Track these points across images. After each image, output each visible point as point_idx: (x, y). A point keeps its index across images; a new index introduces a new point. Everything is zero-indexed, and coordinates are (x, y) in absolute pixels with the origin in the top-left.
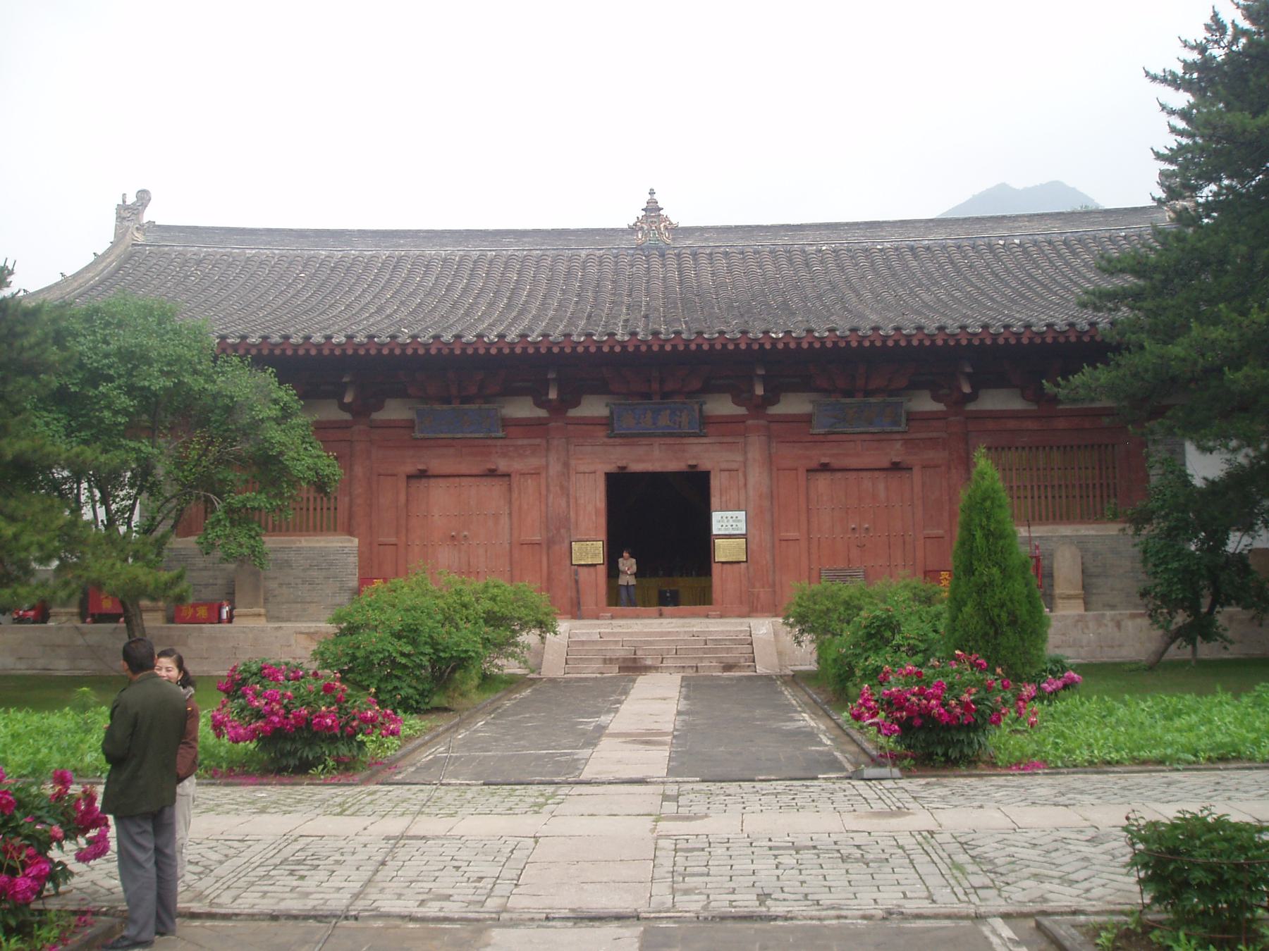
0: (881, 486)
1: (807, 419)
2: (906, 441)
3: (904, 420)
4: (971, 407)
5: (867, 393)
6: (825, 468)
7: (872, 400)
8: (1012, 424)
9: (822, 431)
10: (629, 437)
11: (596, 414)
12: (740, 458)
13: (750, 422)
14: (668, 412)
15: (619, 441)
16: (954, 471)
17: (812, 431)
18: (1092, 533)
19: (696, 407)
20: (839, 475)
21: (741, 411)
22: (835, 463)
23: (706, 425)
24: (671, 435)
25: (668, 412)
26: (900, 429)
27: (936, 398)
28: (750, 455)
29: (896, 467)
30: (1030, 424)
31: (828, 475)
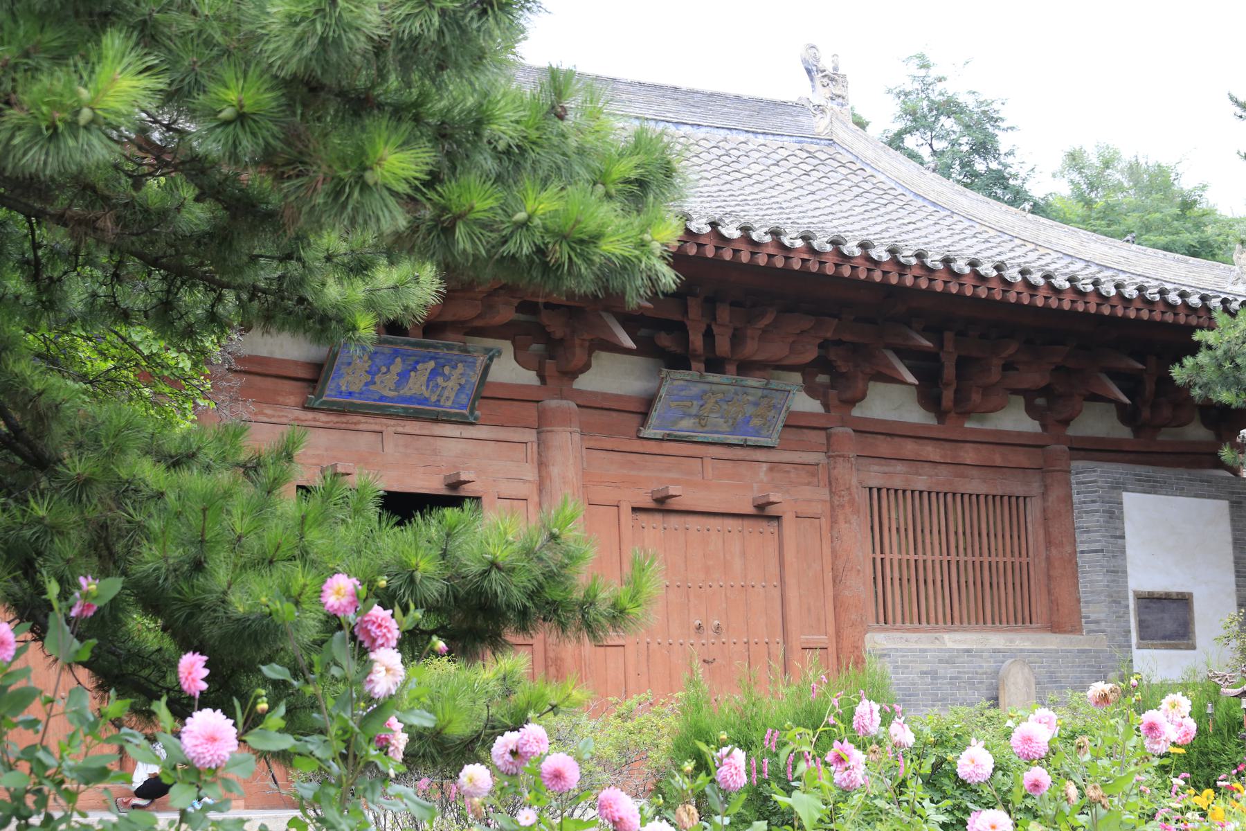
0: (742, 548)
1: (644, 408)
2: (774, 466)
3: (780, 425)
4: (856, 412)
5: (746, 368)
6: (662, 506)
7: (751, 382)
8: (910, 448)
9: (659, 433)
11: (278, 355)
12: (530, 473)
13: (553, 403)
14: (432, 364)
15: (322, 417)
16: (843, 526)
17: (646, 433)
18: (1027, 645)
19: (481, 360)
20: (674, 521)
21: (529, 377)
22: (686, 497)
23: (486, 402)
24: (417, 416)
25: (432, 364)
26: (769, 442)
27: (812, 391)
28: (555, 471)
29: (763, 513)
30: (931, 452)
31: (658, 517)
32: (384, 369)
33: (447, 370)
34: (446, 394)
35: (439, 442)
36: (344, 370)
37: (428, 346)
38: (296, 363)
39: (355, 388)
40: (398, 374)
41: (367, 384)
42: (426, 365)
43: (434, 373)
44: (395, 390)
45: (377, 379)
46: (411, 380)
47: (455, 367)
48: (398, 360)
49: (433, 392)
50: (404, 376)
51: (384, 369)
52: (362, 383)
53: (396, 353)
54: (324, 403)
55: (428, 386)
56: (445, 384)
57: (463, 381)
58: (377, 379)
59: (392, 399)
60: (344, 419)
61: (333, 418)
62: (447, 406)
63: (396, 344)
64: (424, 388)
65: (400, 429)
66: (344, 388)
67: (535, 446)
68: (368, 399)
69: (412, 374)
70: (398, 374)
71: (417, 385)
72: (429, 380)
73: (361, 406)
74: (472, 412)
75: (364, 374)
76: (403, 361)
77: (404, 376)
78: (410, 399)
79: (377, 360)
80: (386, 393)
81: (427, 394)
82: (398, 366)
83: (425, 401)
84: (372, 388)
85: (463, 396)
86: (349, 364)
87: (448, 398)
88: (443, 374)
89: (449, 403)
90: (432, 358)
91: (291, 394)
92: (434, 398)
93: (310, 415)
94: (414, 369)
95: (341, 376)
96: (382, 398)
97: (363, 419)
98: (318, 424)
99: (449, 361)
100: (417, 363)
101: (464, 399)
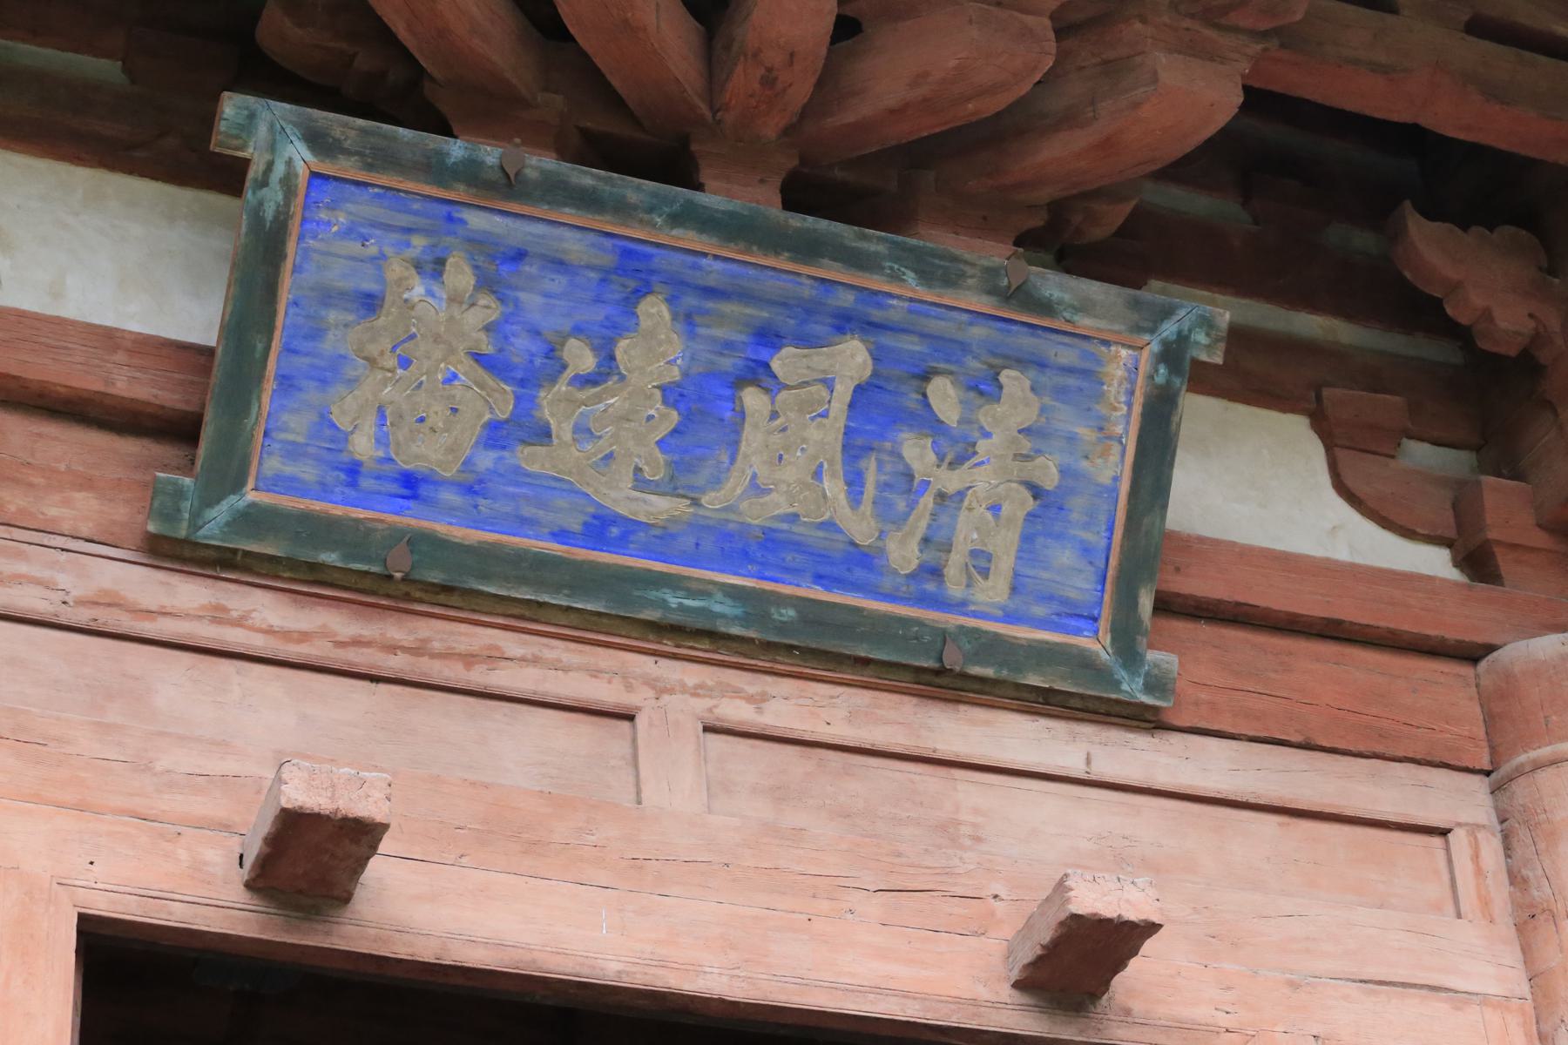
10: (391, 573)
14: (852, 359)
15: (265, 613)
25: (852, 359)
32: (581, 357)
33: (944, 397)
34: (966, 531)
35: (970, 791)
36: (343, 334)
37: (809, 249)
38: (108, 338)
39: (427, 453)
40: (672, 394)
41: (496, 435)
42: (820, 359)
43: (878, 409)
44: (670, 488)
45: (552, 404)
46: (753, 439)
47: (985, 388)
48: (654, 310)
49: (883, 508)
50: (703, 412)
51: (581, 357)
52: (468, 431)
53: (634, 273)
54: (253, 520)
55: (854, 482)
56: (951, 481)
57: (1049, 477)
58: (552, 404)
59: (662, 540)
60: (397, 630)
61: (325, 625)
62: (985, 600)
63: (622, 209)
64: (834, 487)
65: (737, 712)
66: (363, 446)
67: (1491, 848)
68: (524, 523)
69: (752, 399)
70: (672, 394)
71: (788, 460)
72: (854, 449)
73: (487, 559)
74: (1128, 653)
75: (465, 368)
76: (688, 321)
77: (703, 412)
78: (770, 548)
79: (531, 300)
80: (621, 498)
81: (860, 527)
82: (657, 346)
83: (860, 563)
84: (531, 459)
85: (1065, 556)
86: (370, 303)
87: (981, 563)
88: (929, 423)
89: (993, 591)
90: (845, 323)
91: (90, 483)
92: (904, 554)
93: (185, 598)
94: (758, 373)
95: (330, 373)
96: (601, 528)
97: (511, 643)
98: (234, 637)
99: (950, 350)
100: (768, 338)
101: (1073, 572)
